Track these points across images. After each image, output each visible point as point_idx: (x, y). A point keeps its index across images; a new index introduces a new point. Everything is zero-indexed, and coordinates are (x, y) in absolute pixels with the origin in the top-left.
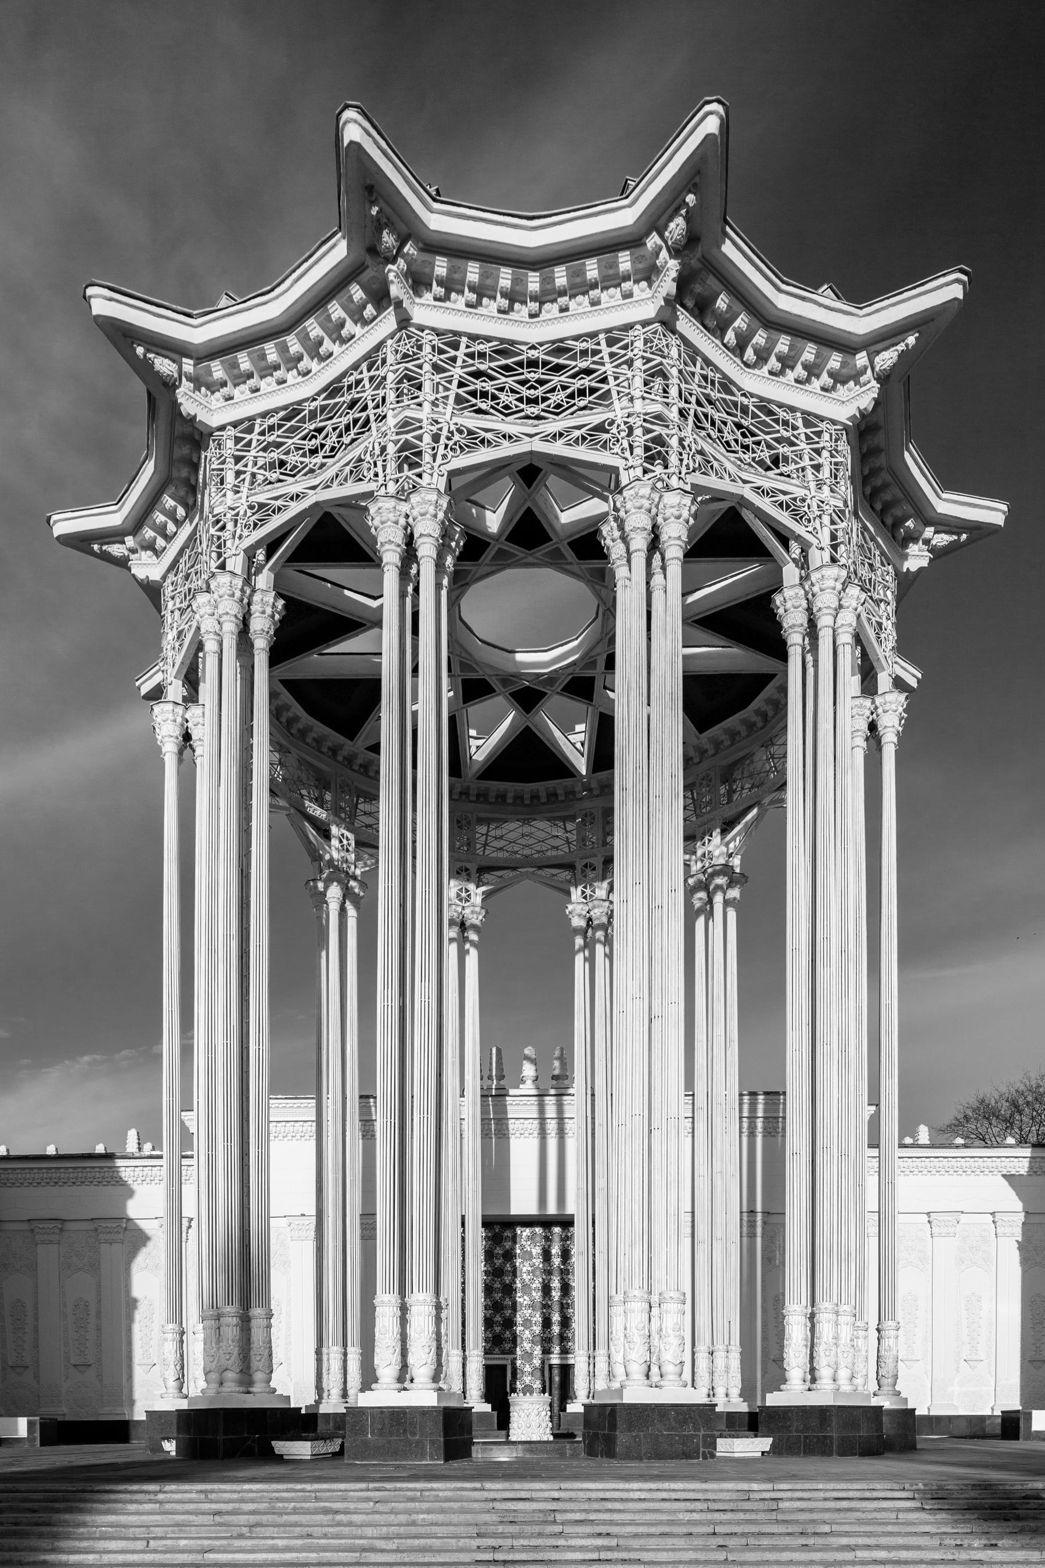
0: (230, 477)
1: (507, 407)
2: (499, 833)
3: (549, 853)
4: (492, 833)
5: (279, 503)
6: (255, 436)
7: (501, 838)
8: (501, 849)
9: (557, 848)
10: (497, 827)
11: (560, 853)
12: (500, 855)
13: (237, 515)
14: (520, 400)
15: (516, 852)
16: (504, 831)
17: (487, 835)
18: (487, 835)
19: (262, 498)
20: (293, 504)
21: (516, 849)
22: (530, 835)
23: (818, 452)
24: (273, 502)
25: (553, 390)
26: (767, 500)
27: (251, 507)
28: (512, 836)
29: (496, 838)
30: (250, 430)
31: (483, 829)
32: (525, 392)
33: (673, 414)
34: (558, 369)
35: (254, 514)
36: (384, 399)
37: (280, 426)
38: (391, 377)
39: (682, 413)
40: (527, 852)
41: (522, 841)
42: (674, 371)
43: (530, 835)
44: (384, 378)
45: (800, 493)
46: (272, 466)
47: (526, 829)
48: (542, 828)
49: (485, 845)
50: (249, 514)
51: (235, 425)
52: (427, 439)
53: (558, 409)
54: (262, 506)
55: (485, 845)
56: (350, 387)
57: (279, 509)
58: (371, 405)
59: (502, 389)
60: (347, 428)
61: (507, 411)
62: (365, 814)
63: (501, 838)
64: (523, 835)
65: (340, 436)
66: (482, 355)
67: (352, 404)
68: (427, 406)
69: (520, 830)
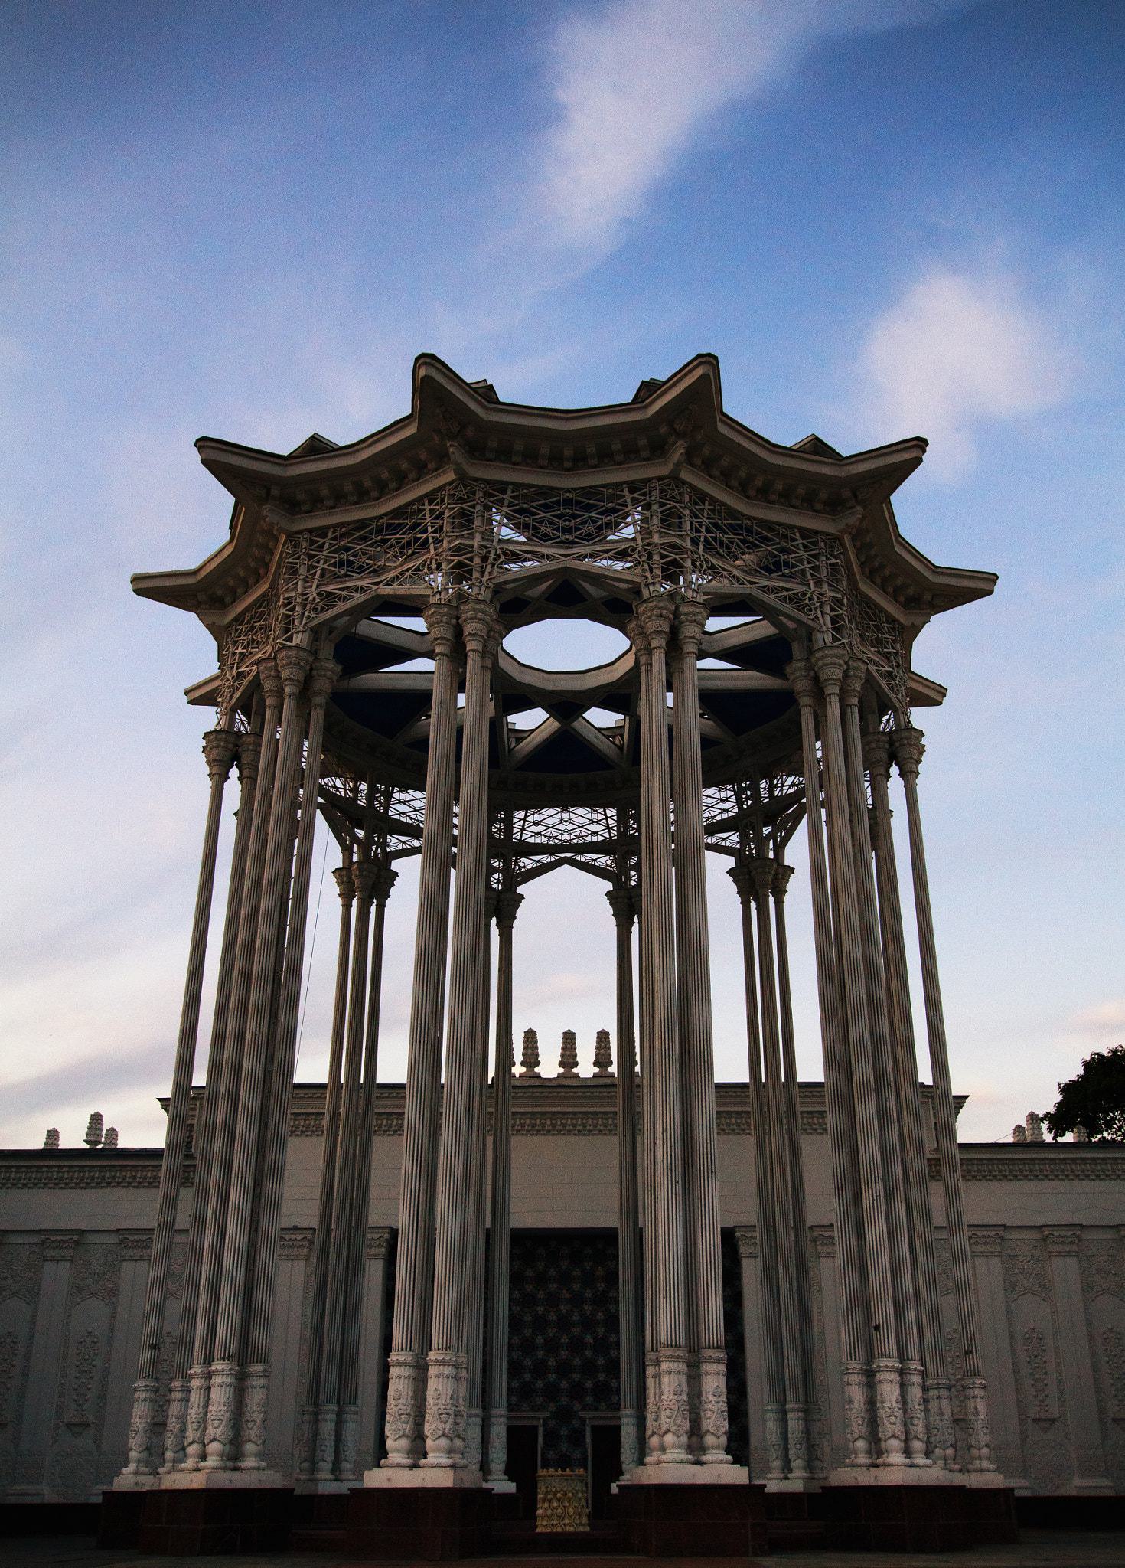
0: (302, 571)
1: (546, 535)
2: (537, 818)
3: (588, 839)
4: (530, 819)
6: (328, 542)
7: (539, 823)
8: (539, 834)
9: (596, 833)
11: (600, 838)
12: (538, 840)
14: (557, 530)
17: (524, 820)
18: (524, 820)
22: (569, 821)
23: (816, 557)
25: (584, 523)
26: (772, 596)
28: (551, 821)
30: (325, 536)
31: (521, 814)
32: (561, 523)
33: (688, 544)
34: (589, 508)
36: (442, 527)
37: (351, 535)
38: (447, 514)
39: (695, 542)
40: (566, 837)
42: (687, 512)
43: (569, 821)
44: (442, 513)
45: (801, 589)
46: (341, 565)
47: (566, 815)
48: (581, 814)
49: (523, 830)
51: (310, 531)
53: (589, 537)
55: (523, 830)
56: (413, 513)
58: (430, 530)
59: (541, 522)
60: (409, 543)
61: (546, 537)
63: (539, 823)
64: (562, 821)
65: (402, 548)
66: (525, 496)
67: (415, 526)
68: (478, 537)
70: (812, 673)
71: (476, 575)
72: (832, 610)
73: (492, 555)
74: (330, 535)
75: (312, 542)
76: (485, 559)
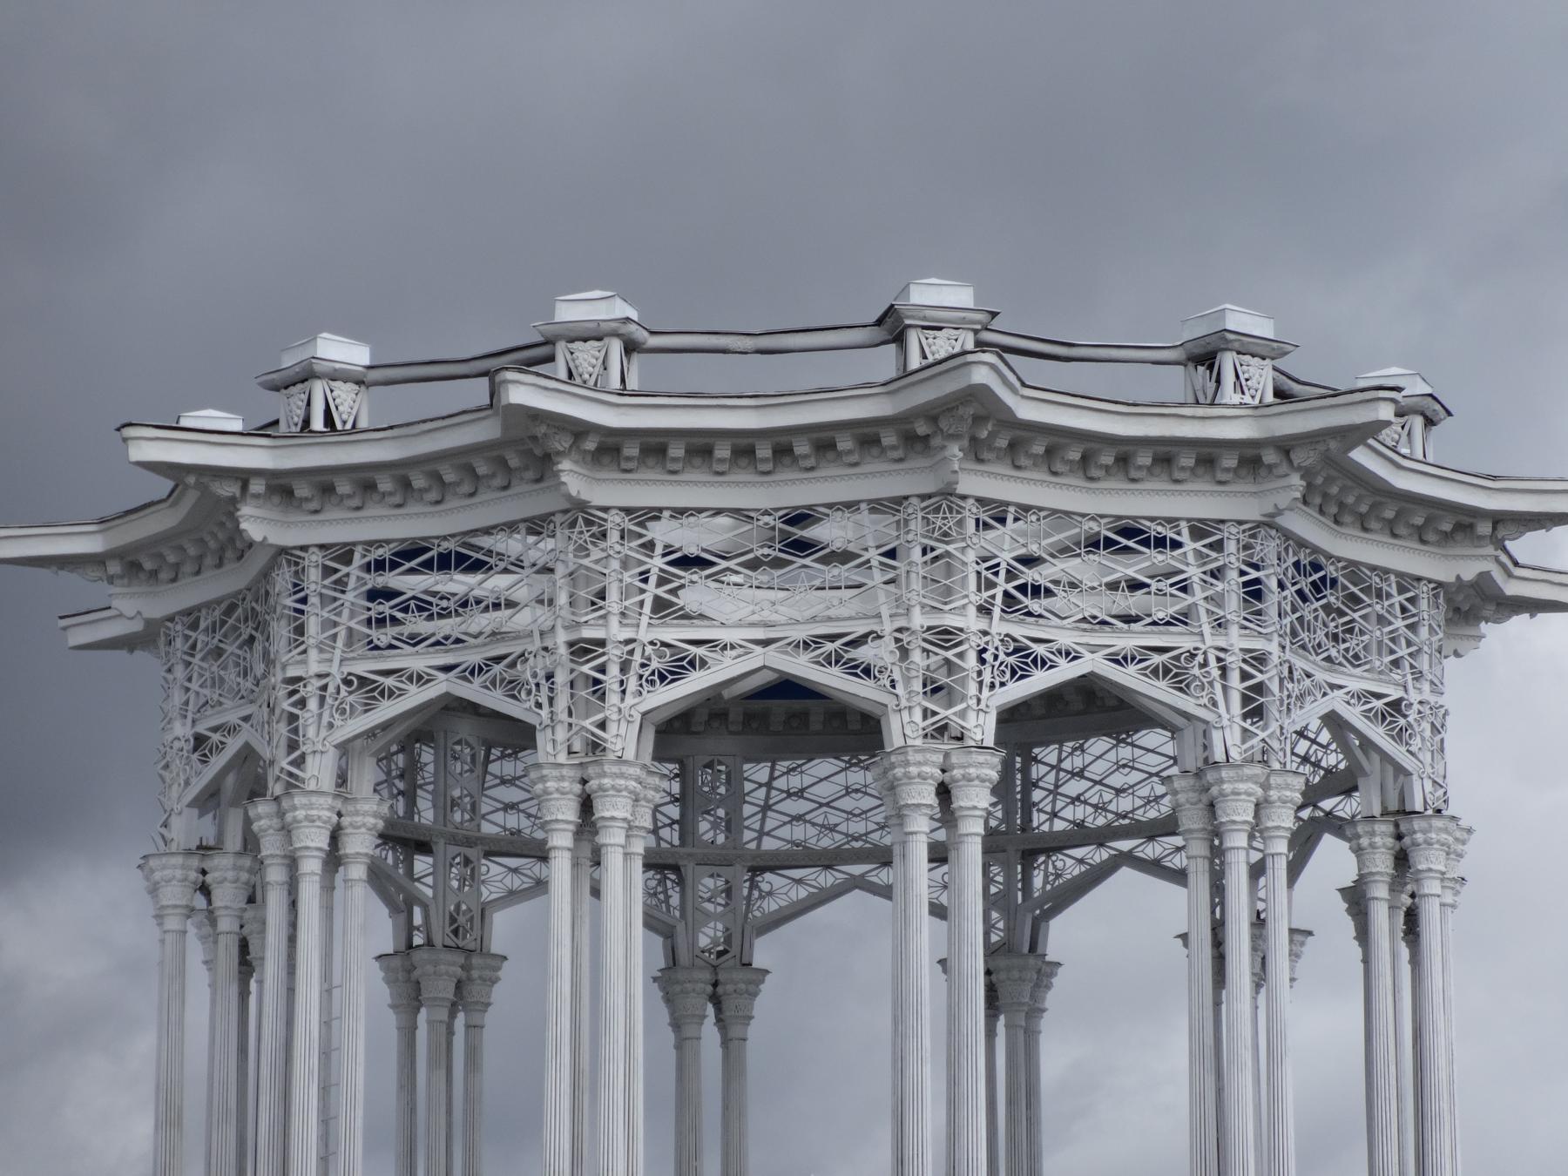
0: (313, 626)
2: (795, 782)
4: (781, 783)
5: (389, 682)
7: (800, 794)
8: (799, 818)
10: (790, 771)
13: (324, 688)
15: (833, 829)
16: (807, 780)
17: (768, 785)
18: (768, 785)
19: (361, 668)
20: (412, 688)
21: (833, 820)
24: (380, 679)
27: (347, 682)
28: (824, 791)
29: (789, 795)
31: (761, 772)
35: (350, 693)
40: (857, 827)
41: (847, 803)
46: (381, 622)
49: (766, 808)
50: (343, 693)
52: (614, 670)
54: (363, 681)
55: (766, 808)
57: (391, 693)
62: (503, 782)
63: (800, 794)
64: (848, 791)
69: (840, 778)
70: (1205, 799)
71: (613, 698)
72: (1245, 676)
73: (637, 658)
74: (358, 560)
75: (328, 571)
76: (625, 667)
